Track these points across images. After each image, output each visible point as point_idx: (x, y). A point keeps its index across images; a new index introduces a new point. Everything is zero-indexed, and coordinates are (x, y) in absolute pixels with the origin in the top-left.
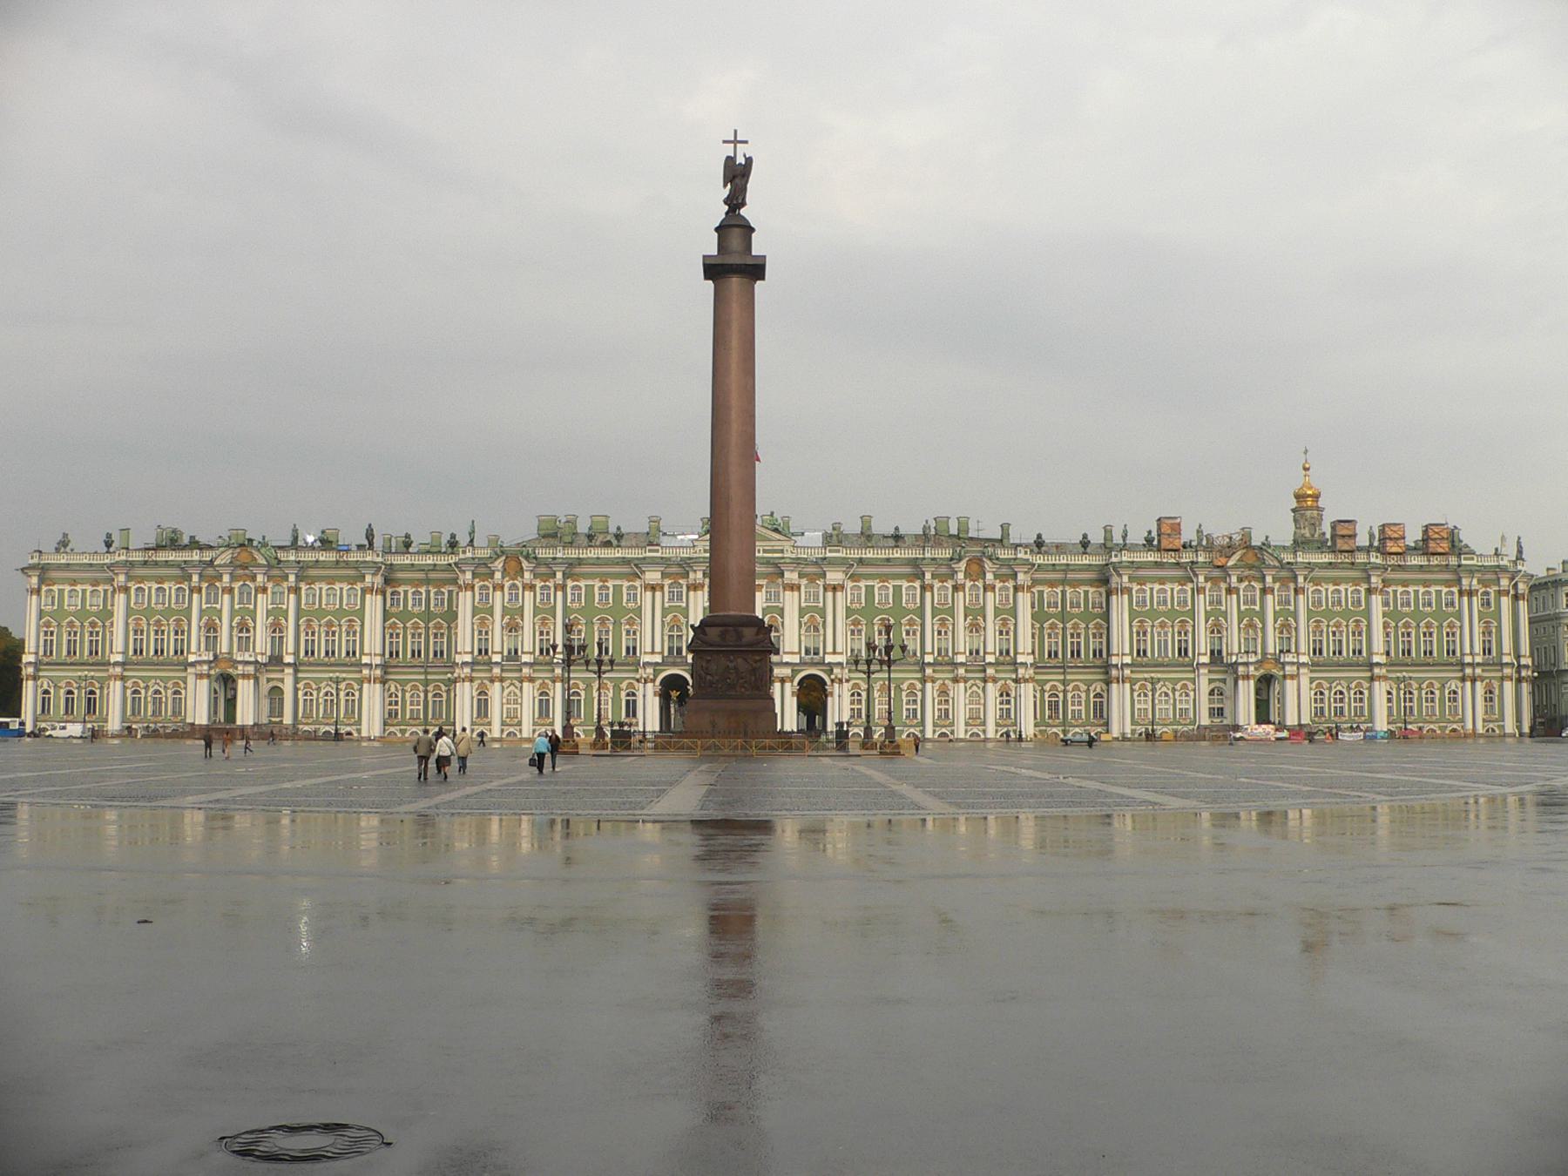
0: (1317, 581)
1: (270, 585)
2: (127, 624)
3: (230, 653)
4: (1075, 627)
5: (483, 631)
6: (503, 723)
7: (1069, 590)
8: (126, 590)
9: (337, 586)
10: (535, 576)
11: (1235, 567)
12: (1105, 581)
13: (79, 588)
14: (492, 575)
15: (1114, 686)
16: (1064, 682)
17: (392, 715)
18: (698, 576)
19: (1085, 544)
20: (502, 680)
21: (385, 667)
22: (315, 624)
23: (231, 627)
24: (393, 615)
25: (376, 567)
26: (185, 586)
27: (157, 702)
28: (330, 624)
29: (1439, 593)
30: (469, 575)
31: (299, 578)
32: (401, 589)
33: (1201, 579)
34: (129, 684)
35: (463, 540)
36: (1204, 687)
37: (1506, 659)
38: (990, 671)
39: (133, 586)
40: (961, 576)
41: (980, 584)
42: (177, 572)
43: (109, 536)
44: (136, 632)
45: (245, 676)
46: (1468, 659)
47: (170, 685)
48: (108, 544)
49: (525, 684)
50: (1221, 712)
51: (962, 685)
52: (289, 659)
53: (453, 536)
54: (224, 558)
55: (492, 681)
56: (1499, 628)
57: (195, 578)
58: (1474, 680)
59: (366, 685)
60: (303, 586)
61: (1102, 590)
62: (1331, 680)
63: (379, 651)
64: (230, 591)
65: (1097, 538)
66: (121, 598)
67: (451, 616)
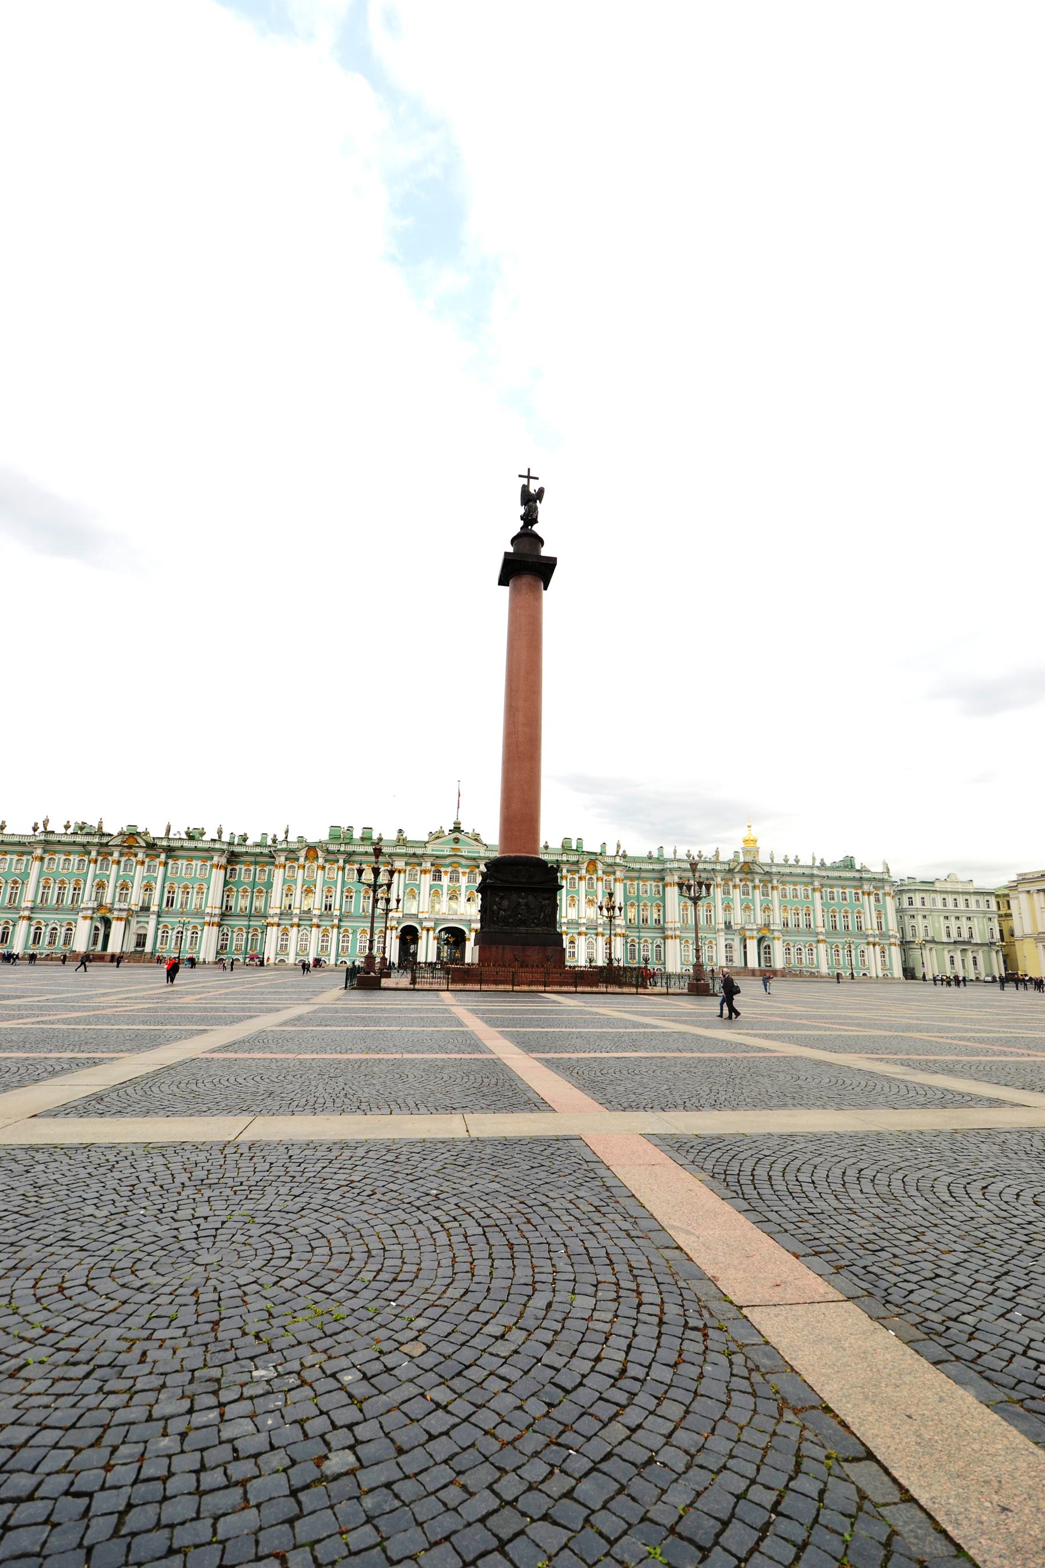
0: (783, 883)
1: (147, 860)
2: (39, 882)
3: (112, 904)
4: (645, 905)
5: (289, 893)
6: (297, 954)
7: (641, 883)
8: (42, 859)
9: (194, 863)
10: (326, 861)
11: (738, 872)
12: (663, 879)
13: (8, 857)
14: (297, 860)
15: (669, 942)
16: (639, 938)
17: (223, 947)
18: (427, 865)
19: (650, 857)
20: (299, 926)
21: (223, 915)
22: (176, 885)
23: (116, 887)
24: (230, 883)
25: (223, 851)
26: (86, 858)
27: (53, 936)
28: (186, 887)
29: (850, 892)
30: (283, 859)
31: (168, 857)
32: (237, 867)
33: (719, 879)
34: (34, 922)
35: (281, 837)
36: (722, 943)
37: (891, 933)
38: (600, 930)
39: (47, 857)
40: (583, 872)
41: (594, 877)
42: (82, 849)
43: (36, 824)
44: (44, 887)
45: (119, 919)
46: (870, 932)
47: (64, 924)
48: (35, 829)
49: (314, 929)
50: (731, 960)
51: (583, 937)
52: (154, 908)
53: (275, 836)
54: (117, 841)
55: (292, 926)
56: (886, 914)
57: (94, 854)
58: (874, 945)
59: (206, 927)
60: (170, 862)
61: (660, 884)
62: (796, 941)
63: (218, 905)
64: (118, 863)
65: (655, 855)
66: (37, 864)
67: (269, 885)
